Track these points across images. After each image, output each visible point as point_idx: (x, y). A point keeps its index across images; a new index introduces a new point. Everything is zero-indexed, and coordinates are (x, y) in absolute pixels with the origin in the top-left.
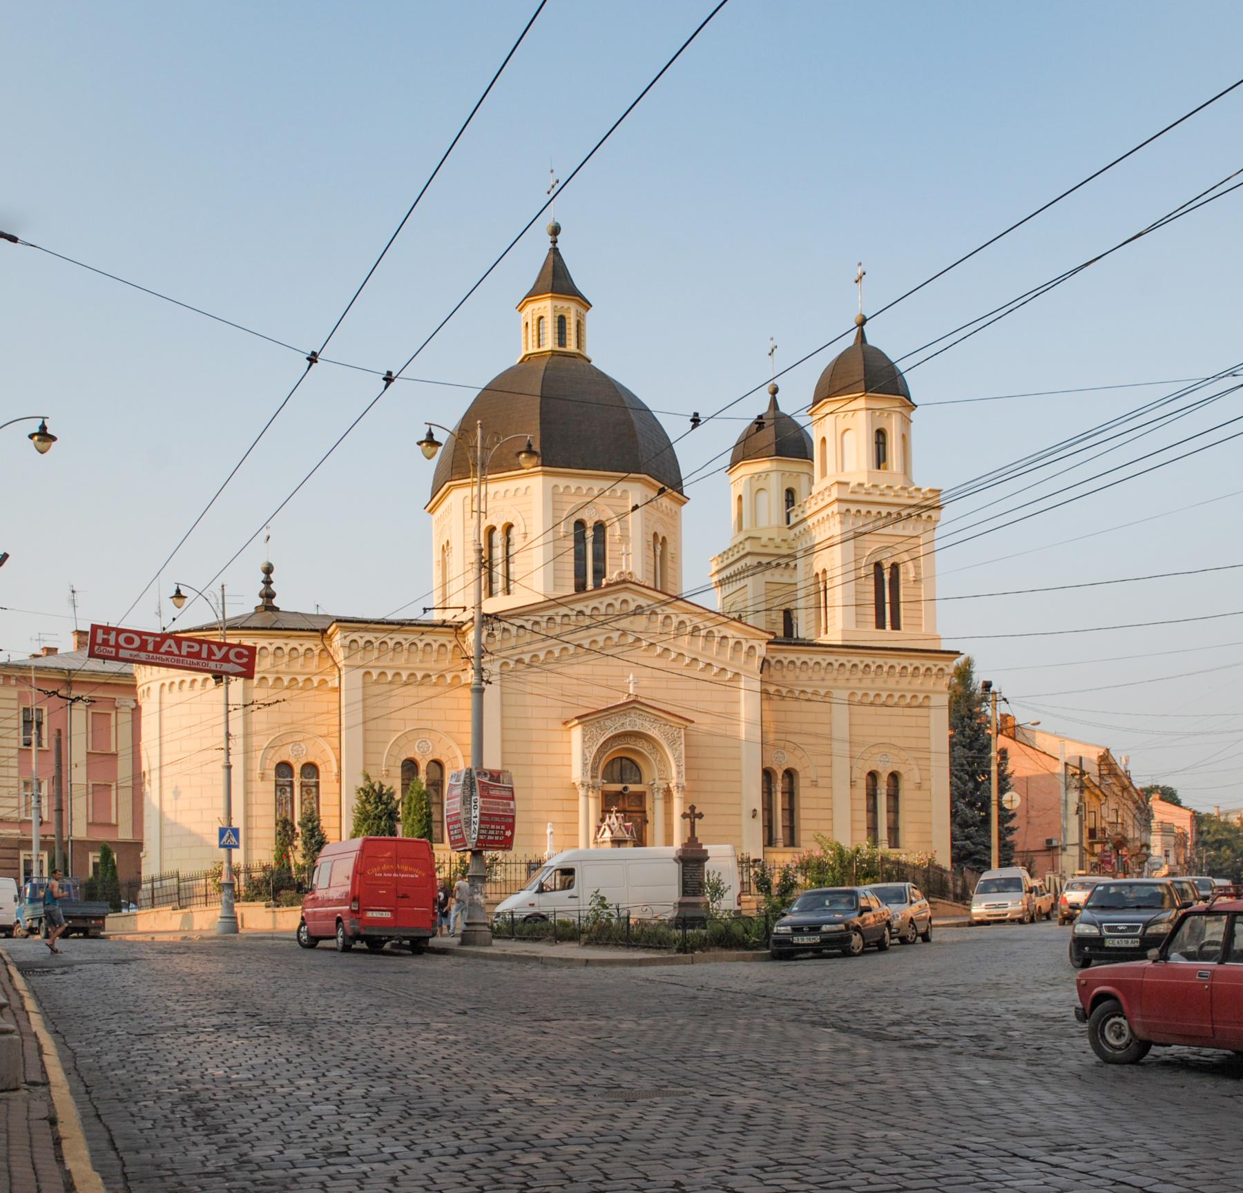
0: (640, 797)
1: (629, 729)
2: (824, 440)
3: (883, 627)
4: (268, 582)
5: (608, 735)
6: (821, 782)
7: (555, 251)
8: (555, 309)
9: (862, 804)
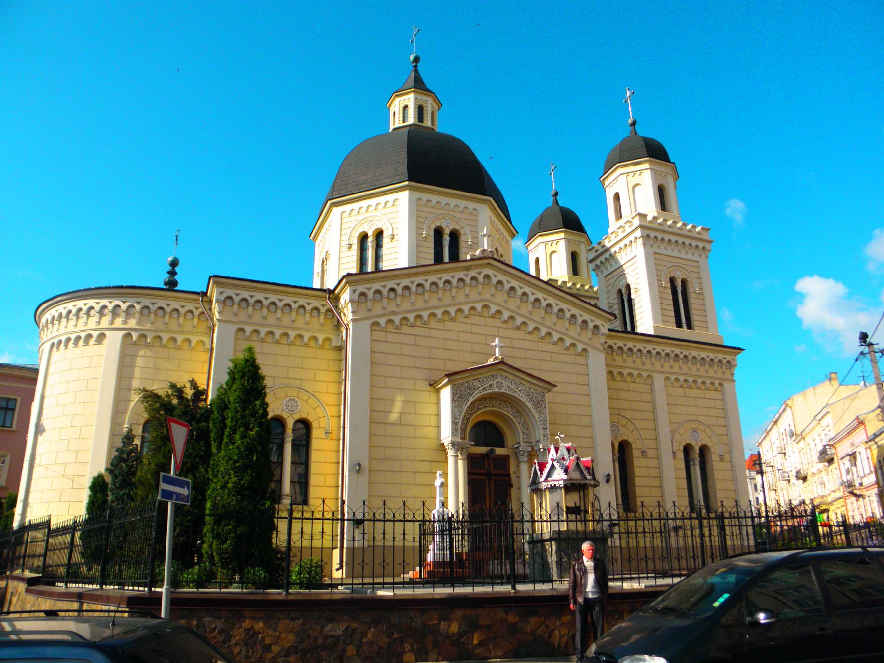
1: (497, 390)
2: (617, 197)
4: (173, 273)
5: (477, 395)
6: (650, 453)
8: (416, 100)
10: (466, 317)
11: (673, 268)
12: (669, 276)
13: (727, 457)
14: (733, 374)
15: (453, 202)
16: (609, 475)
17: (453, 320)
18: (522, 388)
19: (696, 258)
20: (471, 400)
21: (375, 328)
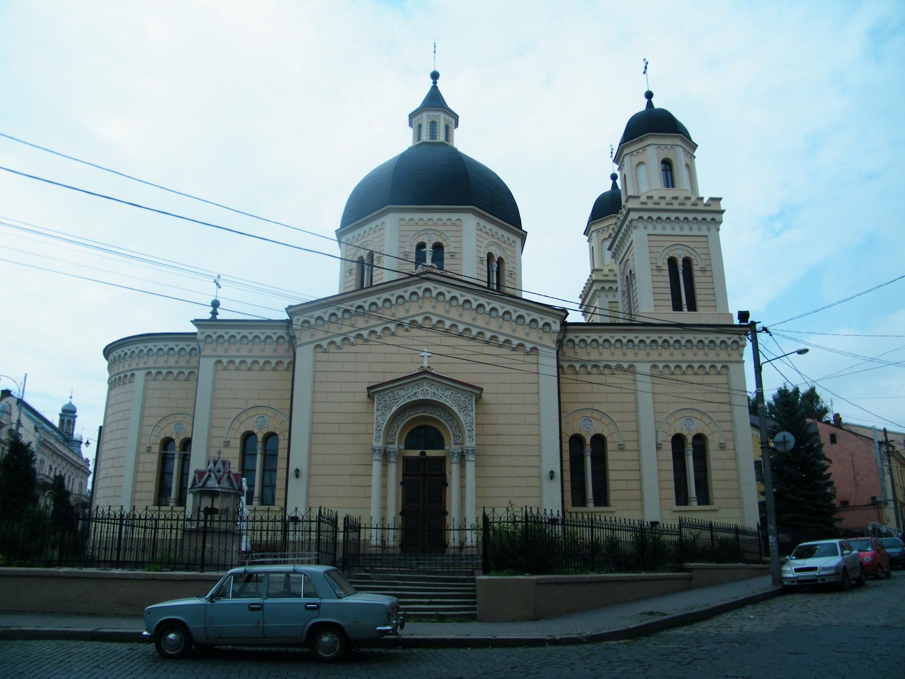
0: (440, 463)
3: (681, 309)
4: (214, 313)
5: (401, 403)
6: (628, 446)
7: (435, 88)
9: (670, 465)
11: (673, 248)
12: (667, 257)
13: (730, 445)
14: (742, 355)
15: (435, 216)
16: (552, 472)
18: (448, 393)
19: (704, 232)
20: (395, 409)
21: (319, 350)
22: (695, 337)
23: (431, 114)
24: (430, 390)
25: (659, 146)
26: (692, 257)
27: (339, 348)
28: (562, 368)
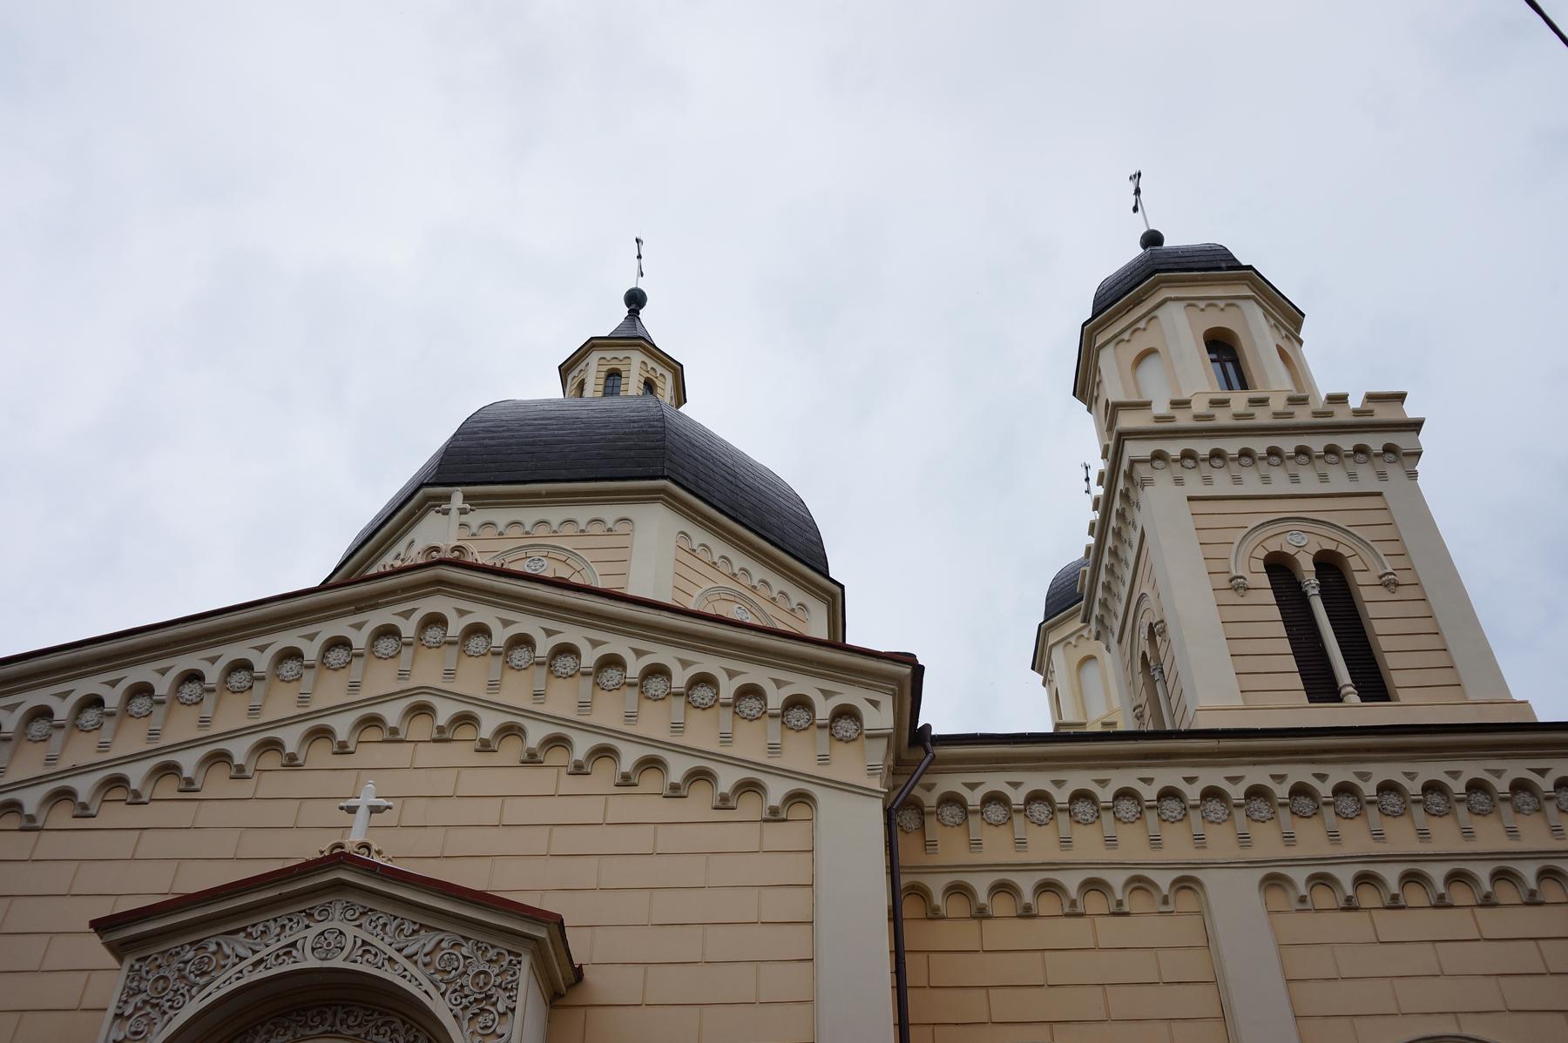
1: (312, 962)
10: (343, 749)
12: (1262, 554)
17: (292, 762)
18: (427, 941)
22: (1416, 774)
23: (609, 354)
24: (350, 930)
25: (1190, 302)
26: (1342, 550)
27: (84, 812)
28: (921, 892)
